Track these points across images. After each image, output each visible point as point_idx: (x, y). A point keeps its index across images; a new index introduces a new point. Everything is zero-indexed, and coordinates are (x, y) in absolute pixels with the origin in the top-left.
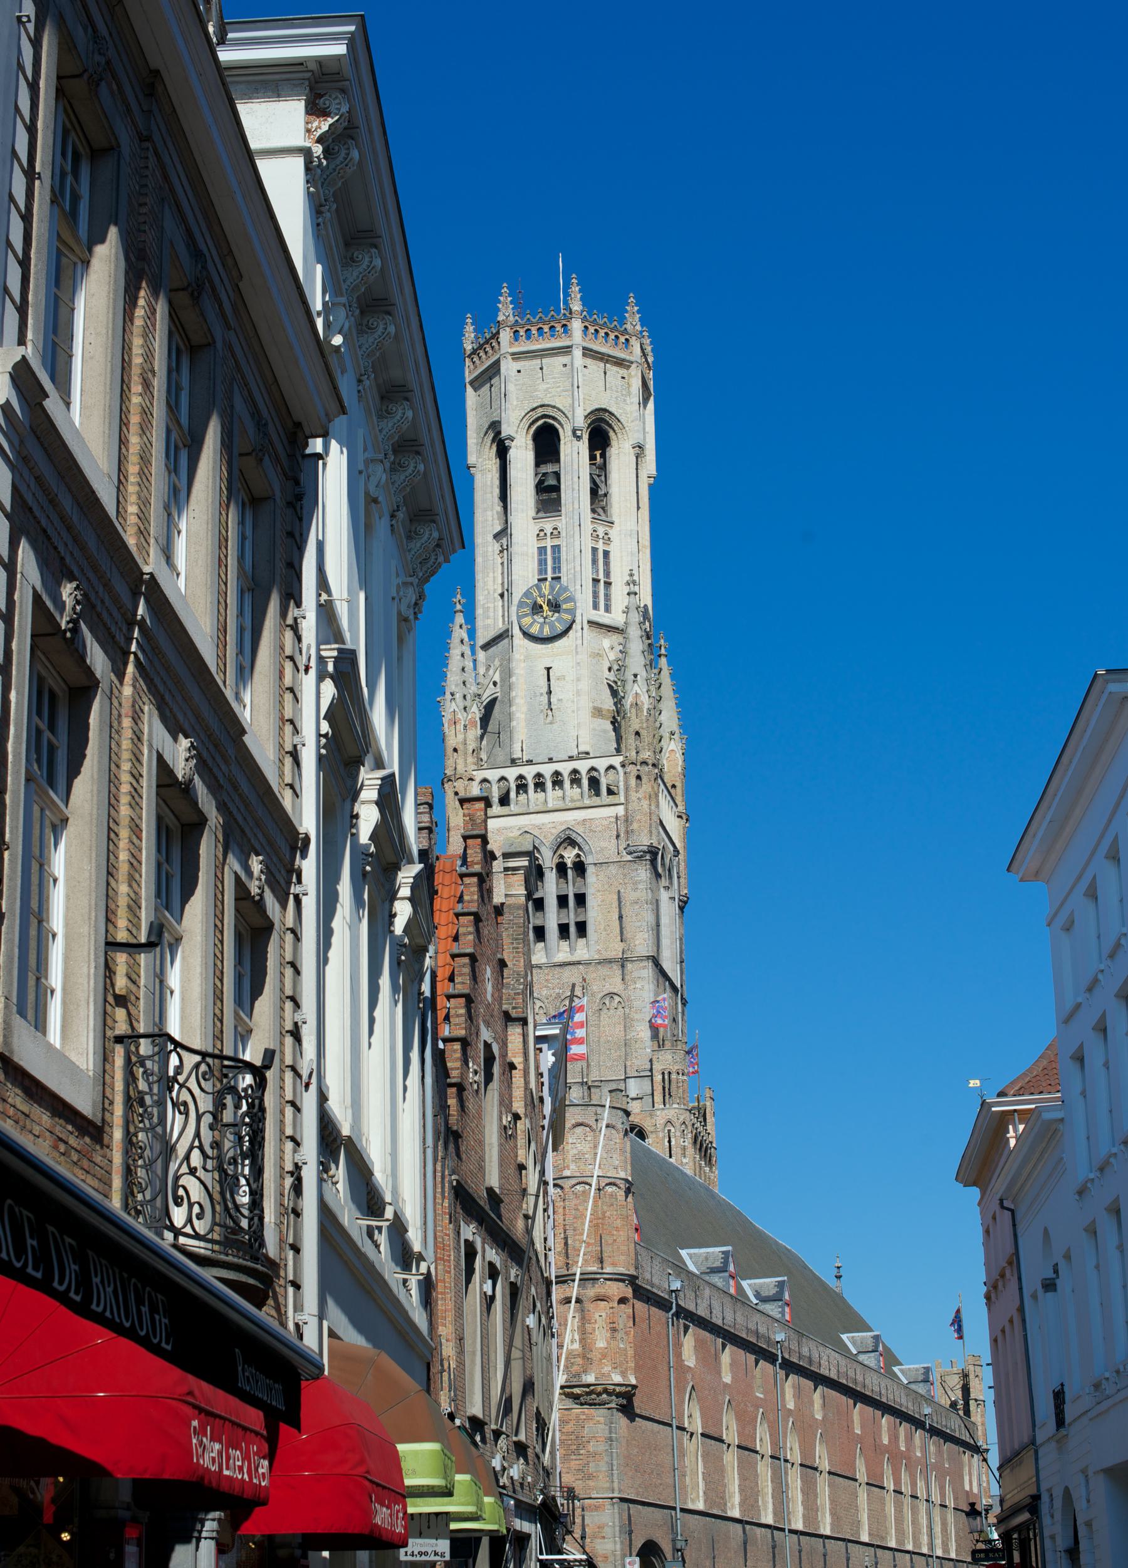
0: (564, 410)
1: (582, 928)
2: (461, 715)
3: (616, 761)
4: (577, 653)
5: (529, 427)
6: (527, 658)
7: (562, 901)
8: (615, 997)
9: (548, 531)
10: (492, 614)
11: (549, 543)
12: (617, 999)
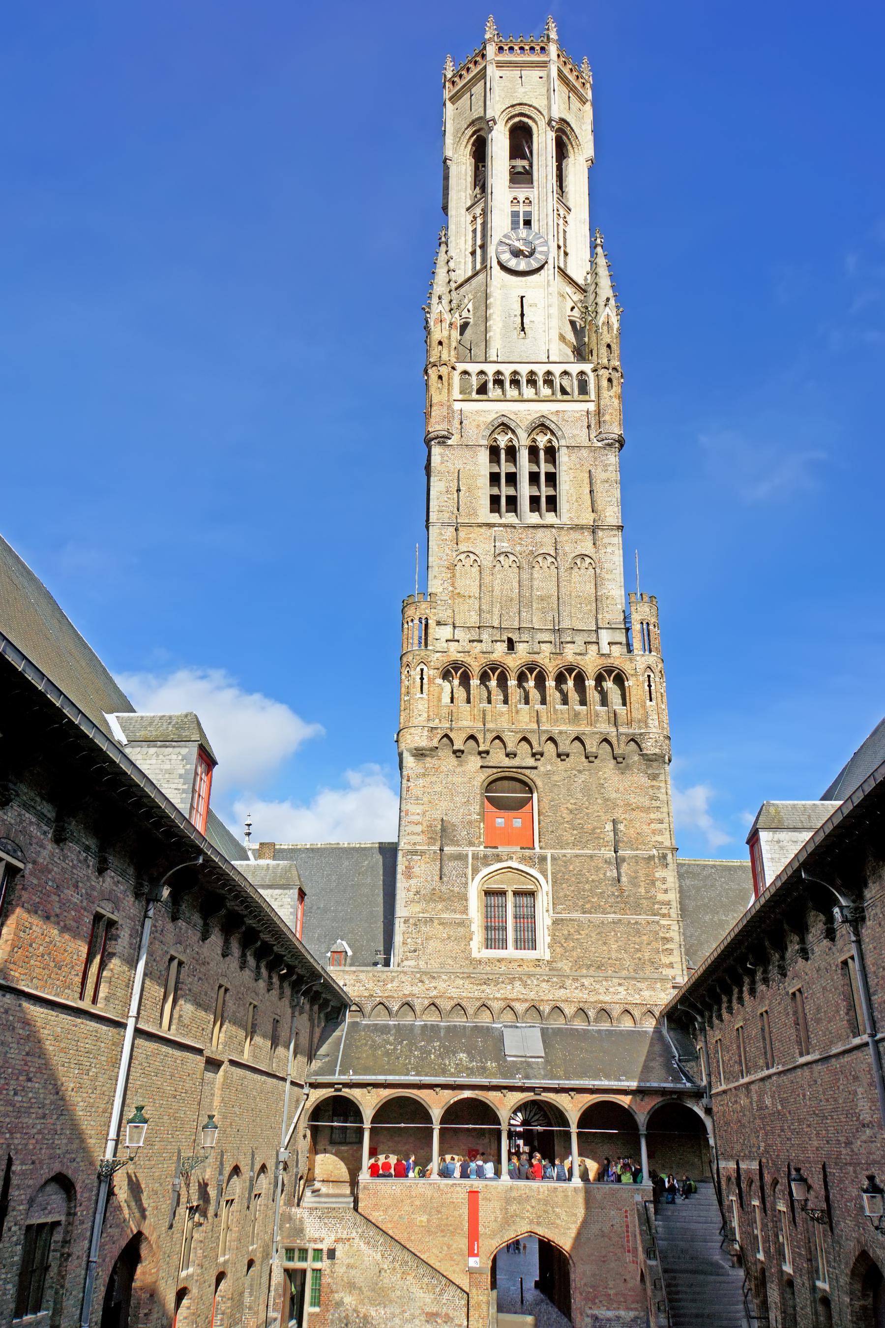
0: (540, 109)
1: (552, 503)
2: (447, 317)
3: (587, 367)
4: (548, 285)
5: (507, 121)
6: (503, 287)
7: (534, 478)
8: (586, 558)
9: (521, 199)
10: (463, 267)
11: (522, 209)
12: (588, 560)
